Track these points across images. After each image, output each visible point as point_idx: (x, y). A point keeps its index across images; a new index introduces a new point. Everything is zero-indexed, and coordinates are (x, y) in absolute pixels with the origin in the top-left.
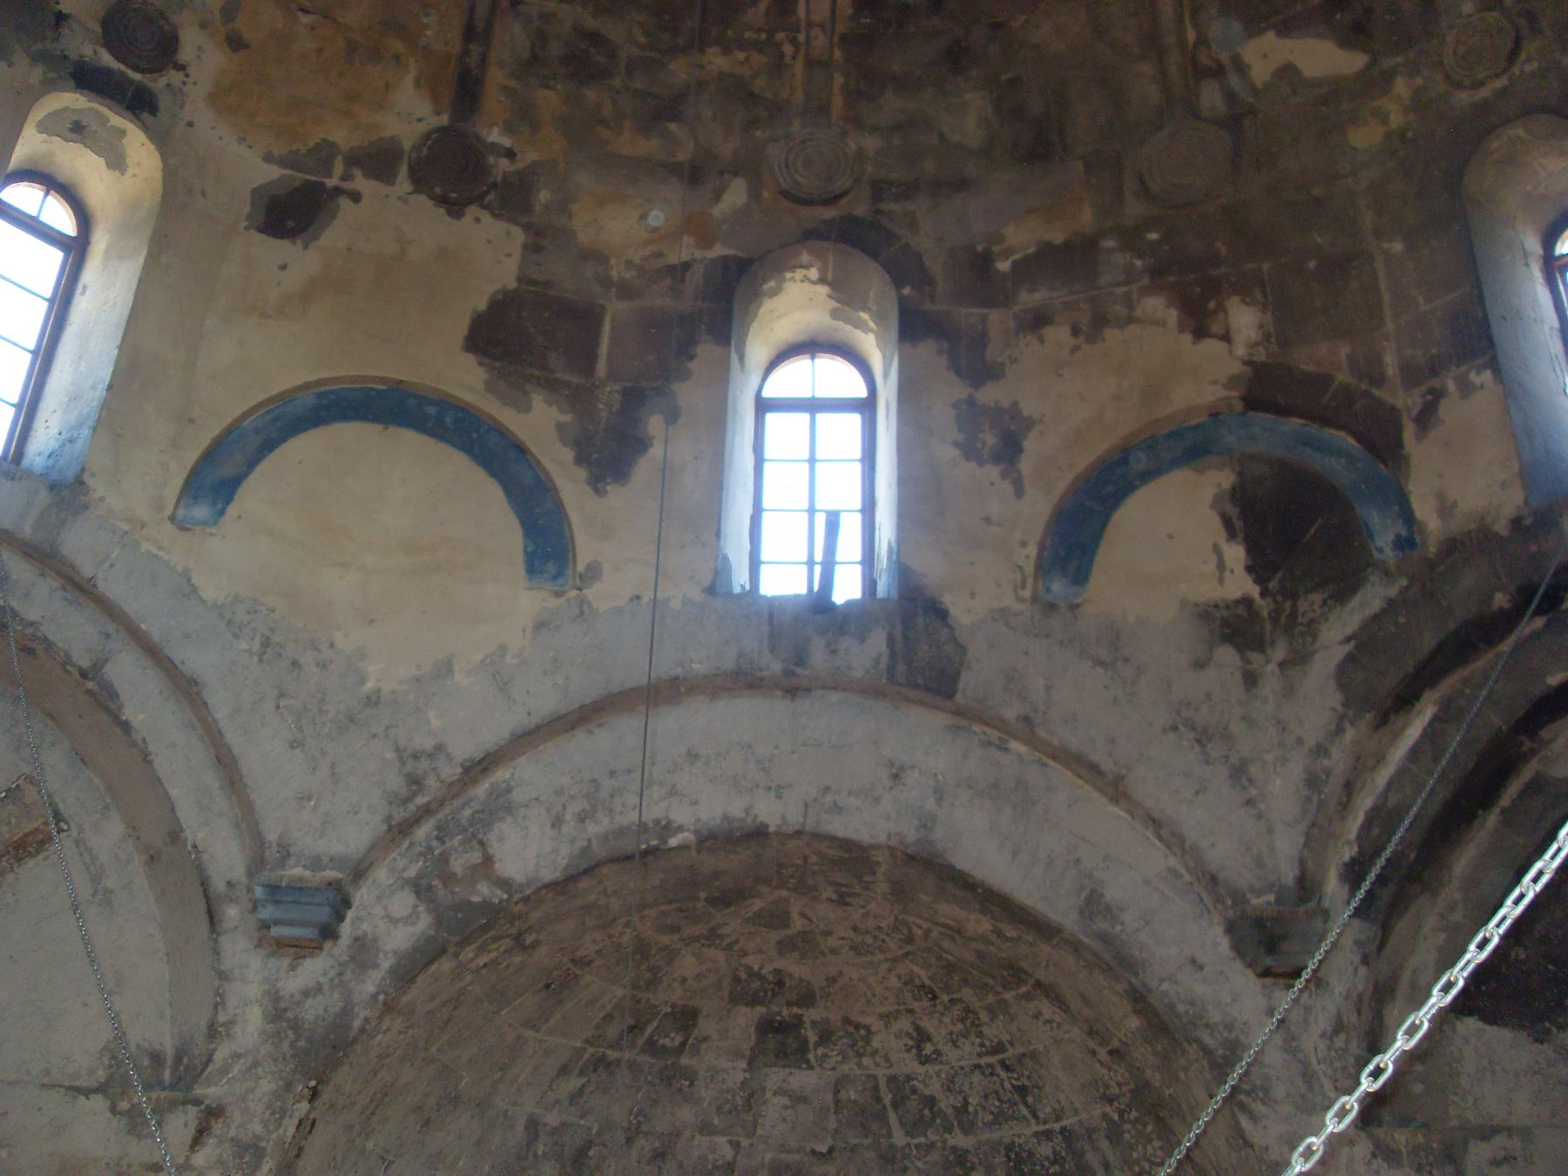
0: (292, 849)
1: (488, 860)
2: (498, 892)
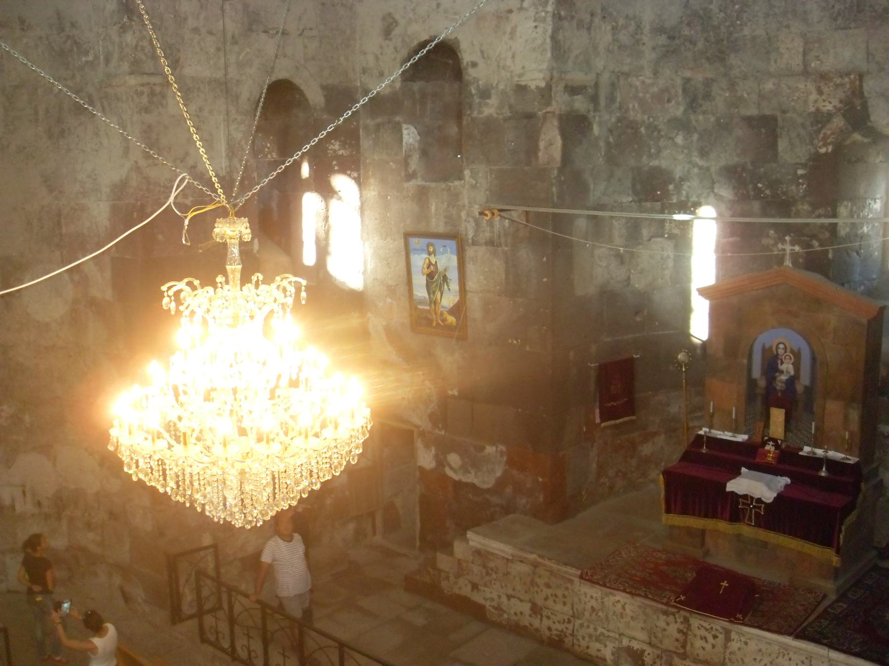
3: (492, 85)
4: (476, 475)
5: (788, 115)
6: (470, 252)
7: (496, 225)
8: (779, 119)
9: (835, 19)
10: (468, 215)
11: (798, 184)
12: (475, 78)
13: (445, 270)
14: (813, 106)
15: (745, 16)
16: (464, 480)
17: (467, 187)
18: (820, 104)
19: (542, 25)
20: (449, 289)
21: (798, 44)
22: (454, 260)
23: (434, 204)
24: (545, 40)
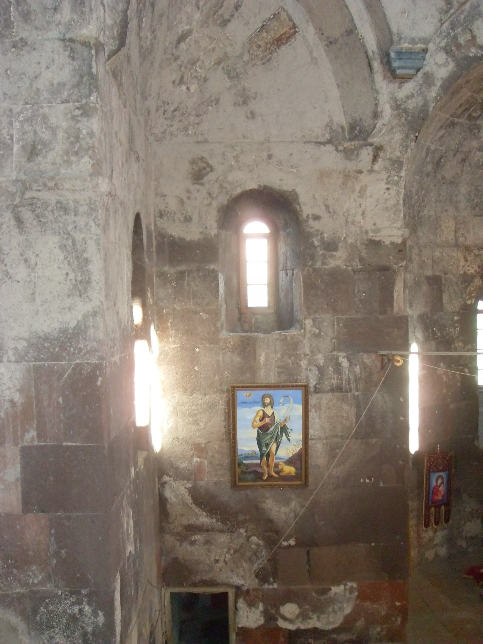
0: (402, 36)
1: (474, 37)
2: (480, 51)
3: (340, 238)
4: (318, 617)
5: (448, 276)
6: (313, 400)
7: (345, 372)
8: (443, 278)
9: (474, 209)
10: (310, 363)
11: (455, 327)
12: (318, 231)
13: (285, 420)
14: (462, 270)
15: (426, 199)
16: (302, 627)
17: (308, 335)
18: (466, 268)
19: (395, 188)
20: (289, 440)
21: (451, 224)
22: (298, 410)
23: (263, 355)
24: (398, 201)
